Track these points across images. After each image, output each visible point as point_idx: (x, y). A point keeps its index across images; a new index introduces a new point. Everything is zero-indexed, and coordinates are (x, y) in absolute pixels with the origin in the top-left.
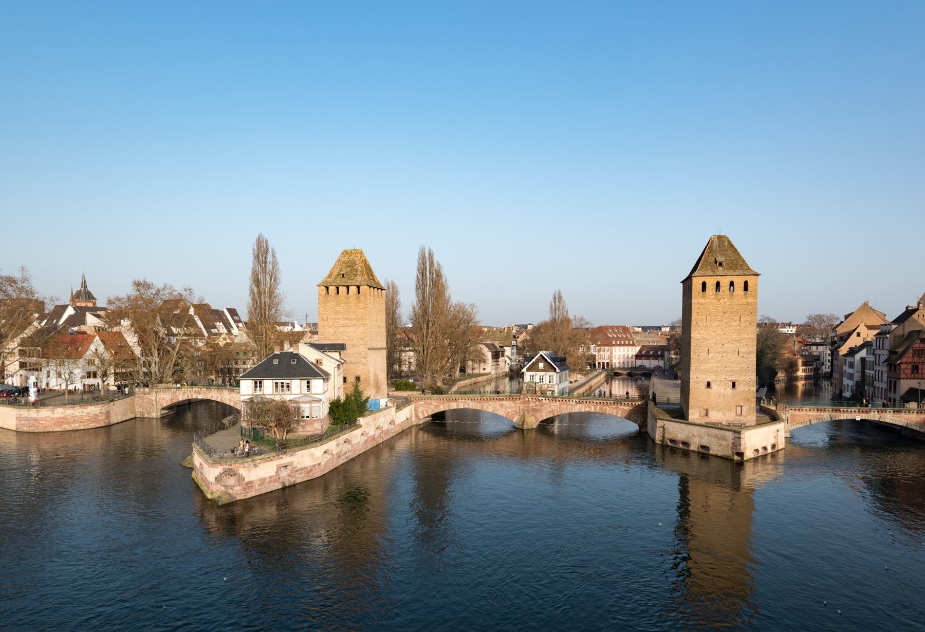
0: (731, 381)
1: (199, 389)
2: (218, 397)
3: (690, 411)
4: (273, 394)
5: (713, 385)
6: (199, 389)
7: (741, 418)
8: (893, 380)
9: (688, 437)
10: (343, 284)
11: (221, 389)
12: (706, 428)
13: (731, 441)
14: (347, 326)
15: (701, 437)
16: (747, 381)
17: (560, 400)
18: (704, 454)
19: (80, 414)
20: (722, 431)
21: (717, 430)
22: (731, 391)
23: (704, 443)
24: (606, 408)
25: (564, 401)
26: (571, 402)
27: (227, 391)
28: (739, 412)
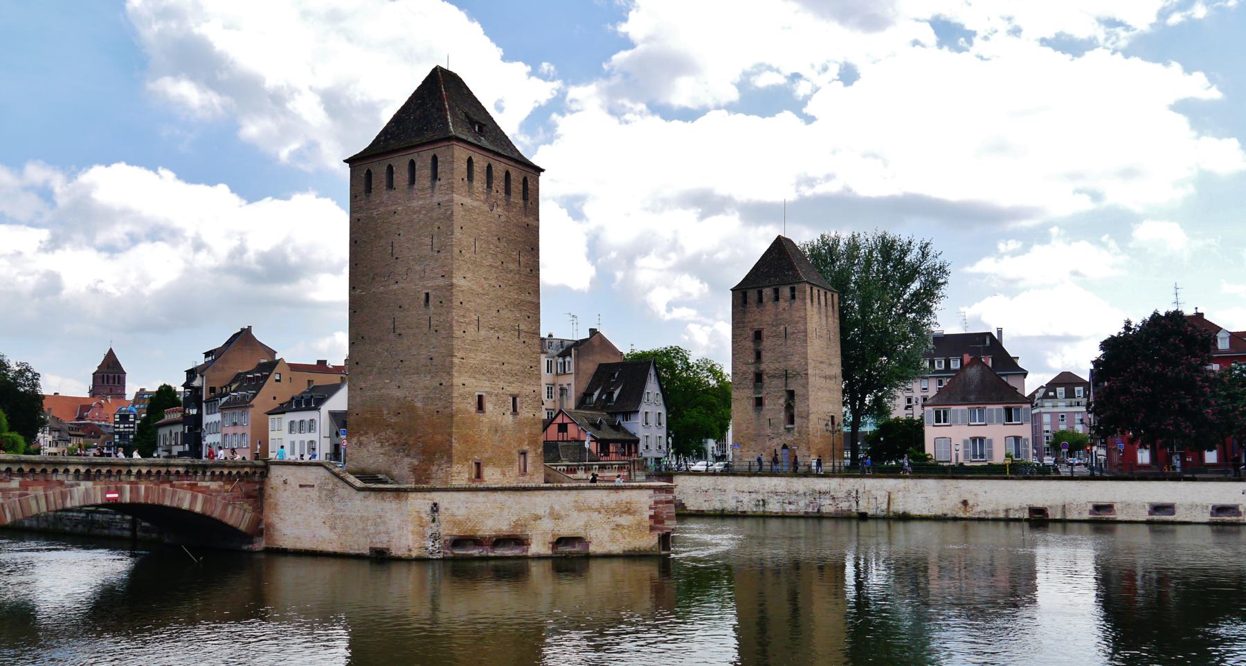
0: (510, 395)
5: (488, 406)
7: (527, 478)
9: (516, 525)
12: (574, 492)
13: (648, 513)
15: (555, 516)
16: (531, 396)
17: (26, 469)
20: (621, 492)
21: (607, 491)
22: (511, 417)
23: (566, 530)
24: (164, 490)
25: (38, 470)
26: (61, 477)
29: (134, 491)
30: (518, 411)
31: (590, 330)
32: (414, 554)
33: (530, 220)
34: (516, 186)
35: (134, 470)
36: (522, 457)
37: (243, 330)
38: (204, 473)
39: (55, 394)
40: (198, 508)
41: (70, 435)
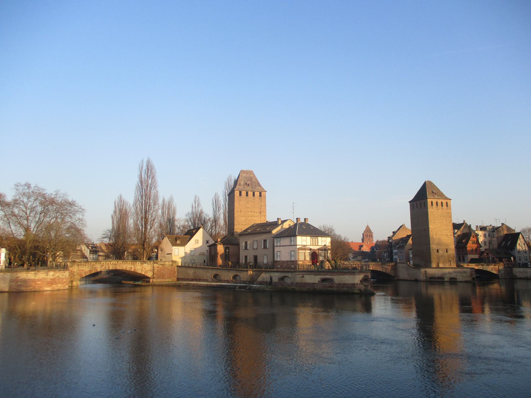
1: (116, 262)
2: (131, 268)
3: (432, 264)
4: (310, 245)
6: (116, 262)
8: (461, 256)
10: (251, 190)
11: (136, 262)
13: (469, 273)
14: (254, 217)
18: (453, 281)
19: (62, 277)
27: (140, 263)
28: (450, 264)
29: (373, 268)
30: (448, 252)
31: (502, 223)
32: (422, 280)
33: (449, 211)
34: (444, 204)
35: (372, 264)
36: (450, 262)
37: (403, 225)
38: (385, 265)
39: (352, 242)
40: (384, 271)
41: (358, 255)
